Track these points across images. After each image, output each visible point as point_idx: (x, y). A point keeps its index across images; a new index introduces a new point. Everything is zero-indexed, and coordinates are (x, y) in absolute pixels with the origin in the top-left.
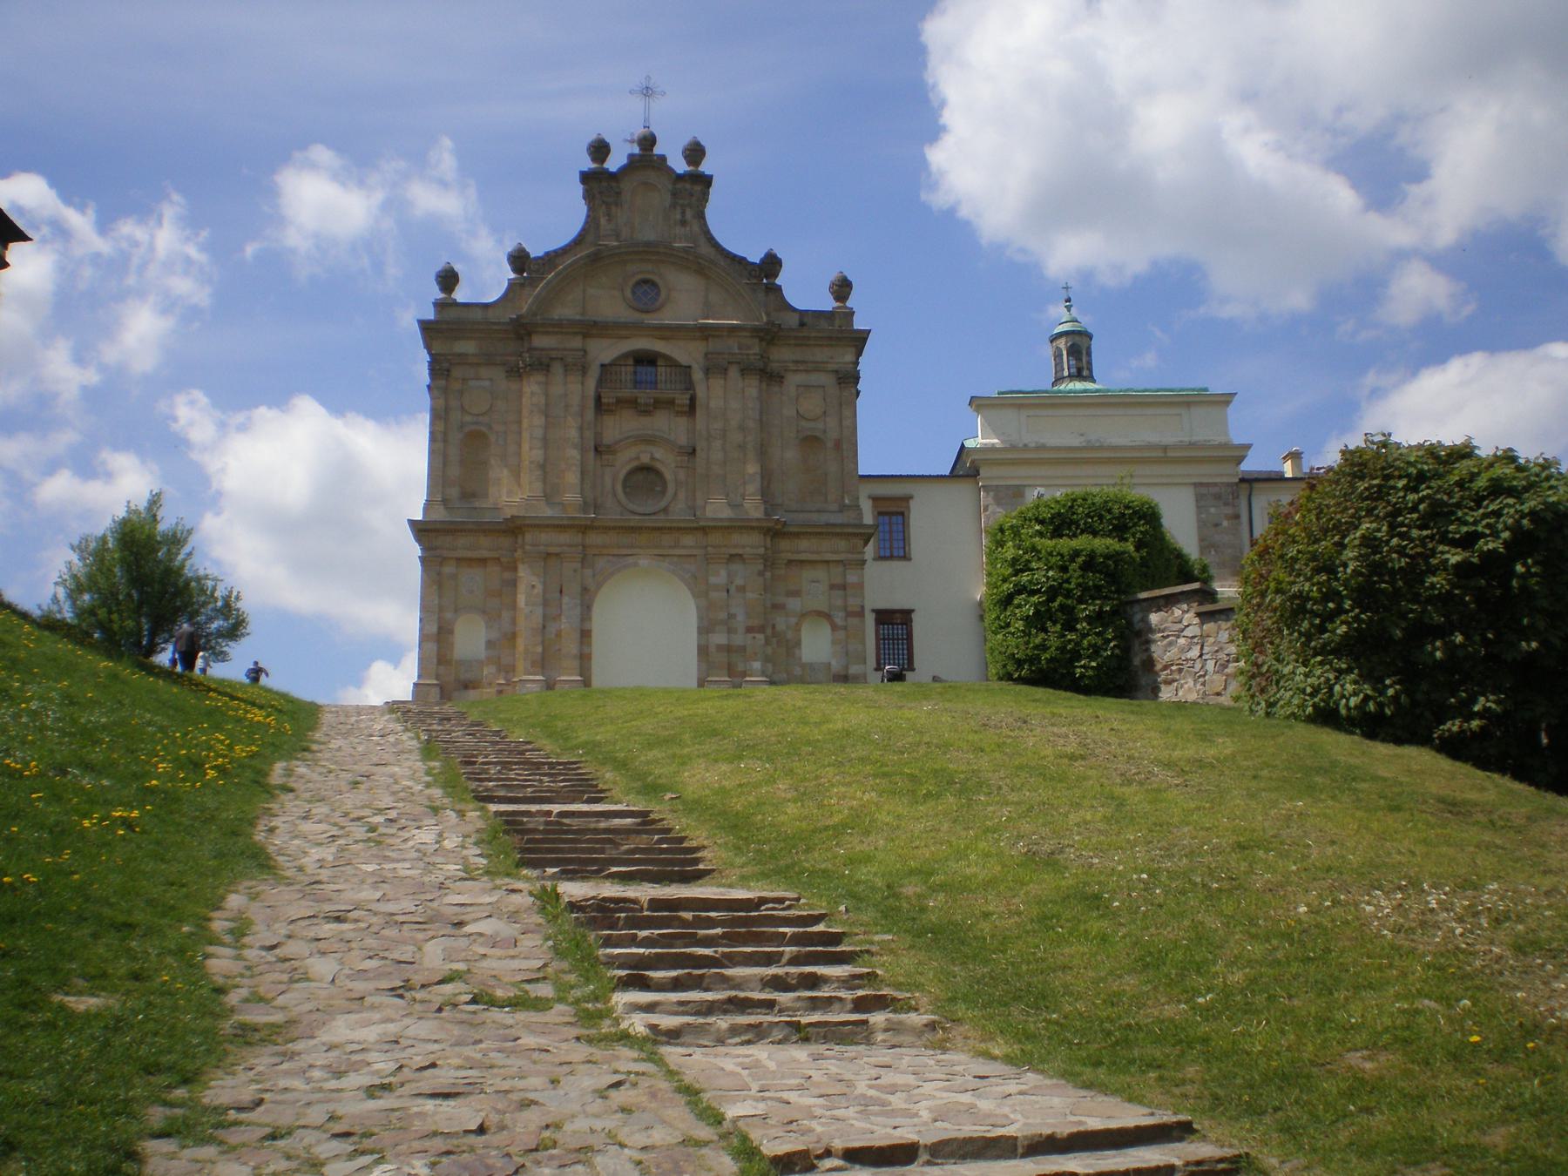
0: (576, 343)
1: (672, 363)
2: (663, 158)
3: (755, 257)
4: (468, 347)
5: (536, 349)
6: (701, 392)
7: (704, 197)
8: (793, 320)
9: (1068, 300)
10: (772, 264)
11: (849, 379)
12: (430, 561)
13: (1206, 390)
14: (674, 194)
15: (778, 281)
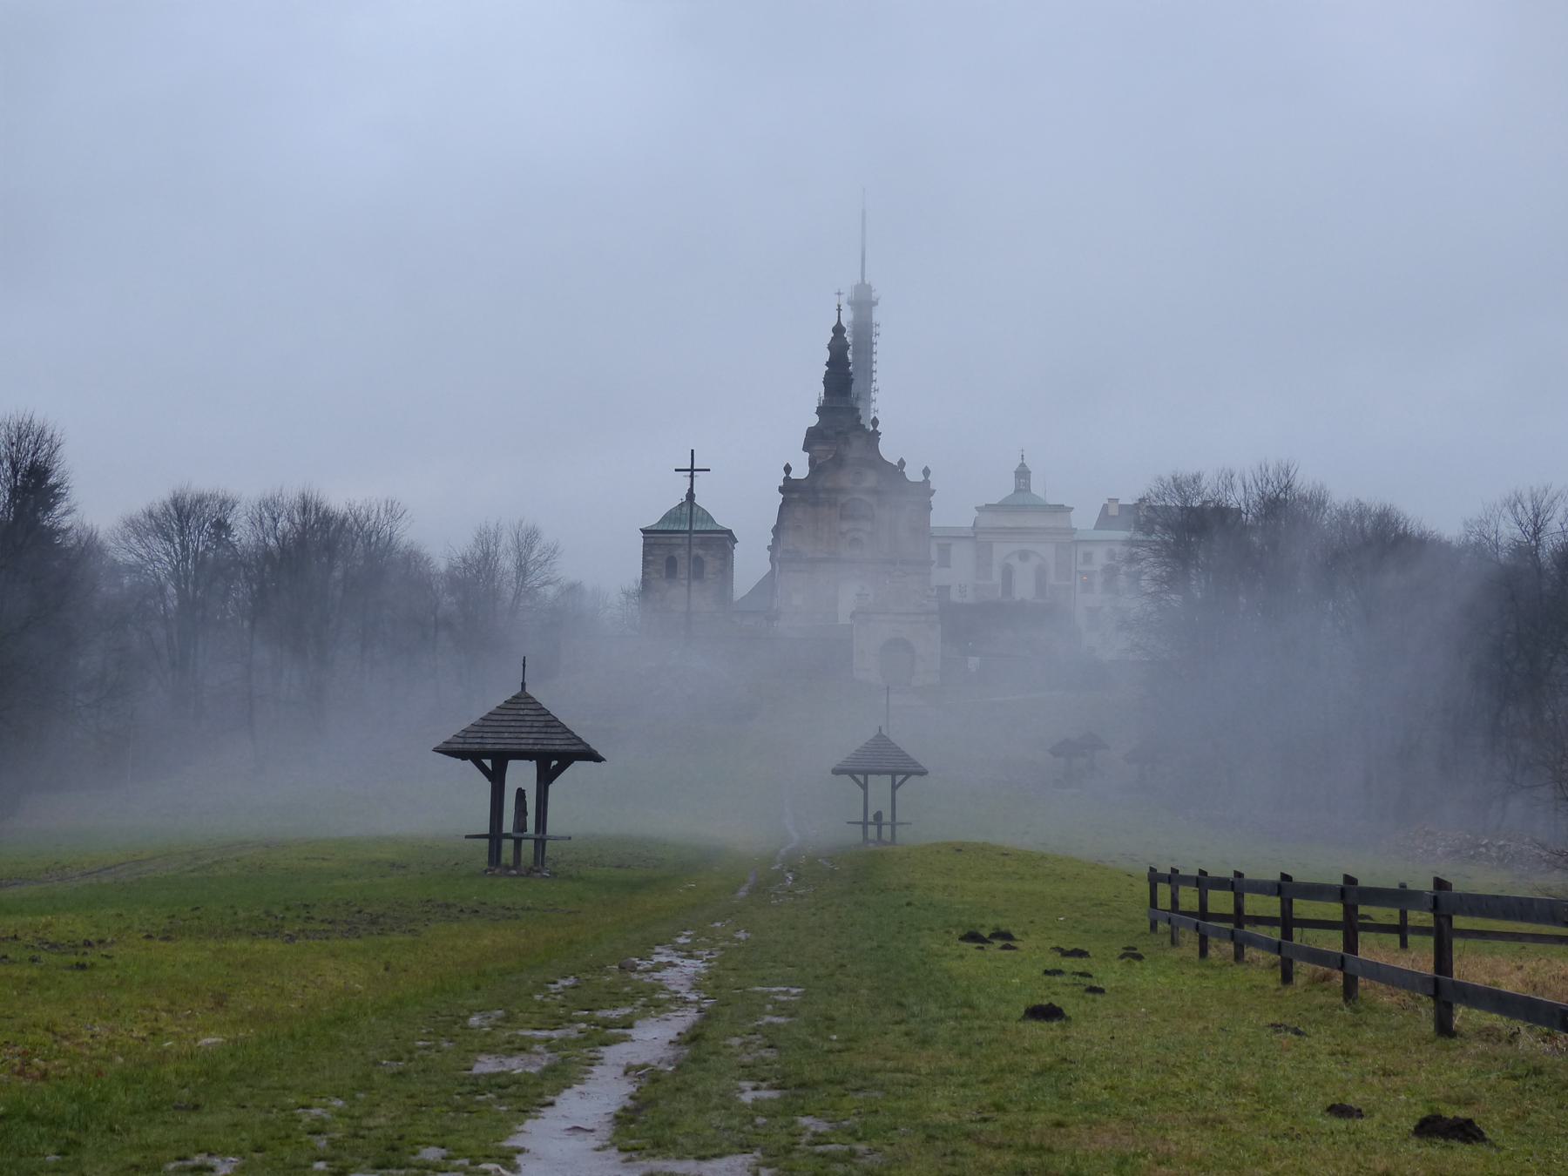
9: (1022, 456)
10: (902, 463)
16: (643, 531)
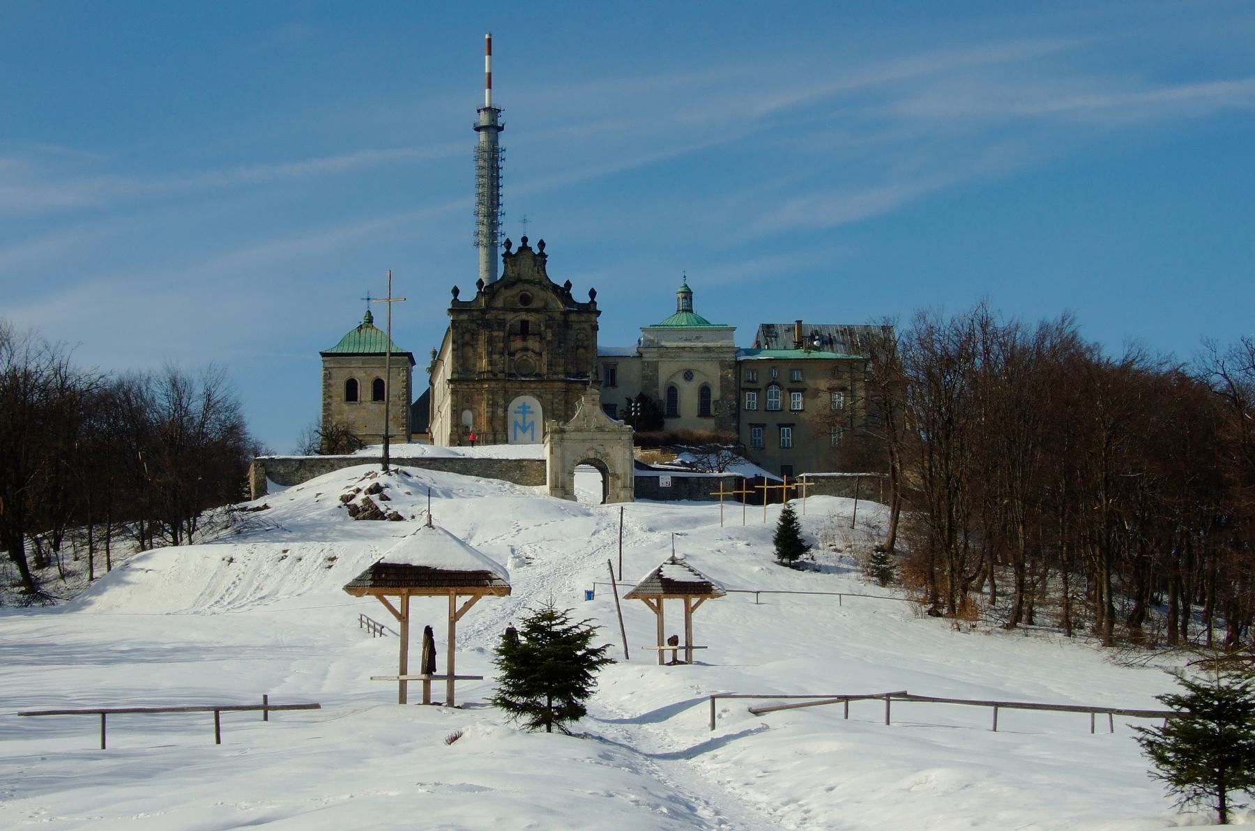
2: (530, 249)
3: (562, 286)
4: (464, 317)
9: (685, 277)
10: (568, 285)
11: (595, 328)
12: (454, 392)
13: (726, 325)
14: (535, 261)
16: (323, 355)
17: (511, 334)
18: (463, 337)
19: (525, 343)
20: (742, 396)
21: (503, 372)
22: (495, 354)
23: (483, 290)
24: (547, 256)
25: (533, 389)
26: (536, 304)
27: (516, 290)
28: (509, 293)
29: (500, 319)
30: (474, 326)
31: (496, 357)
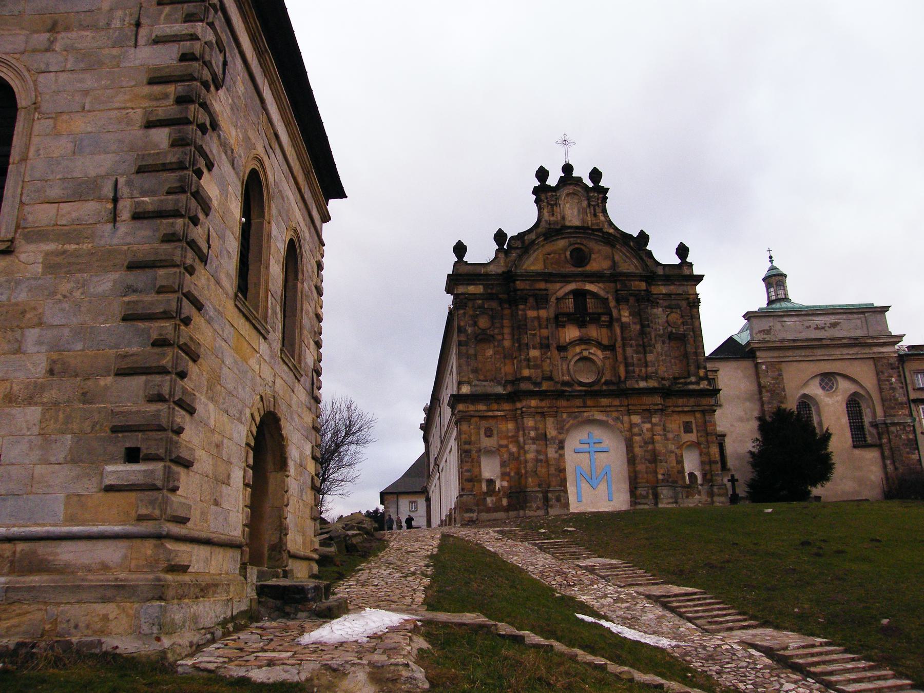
0: (542, 285)
1: (594, 295)
2: (579, 179)
5: (519, 290)
6: (615, 313)
7: (605, 199)
8: (660, 271)
9: (771, 257)
14: (589, 199)
15: (648, 248)
17: (560, 320)
18: (475, 324)
19: (584, 330)
20: (914, 413)
21: (550, 378)
22: (534, 348)
23: (505, 247)
24: (606, 190)
25: (607, 406)
26: (597, 264)
27: (561, 243)
28: (549, 248)
29: (540, 290)
30: (494, 304)
31: (534, 353)
